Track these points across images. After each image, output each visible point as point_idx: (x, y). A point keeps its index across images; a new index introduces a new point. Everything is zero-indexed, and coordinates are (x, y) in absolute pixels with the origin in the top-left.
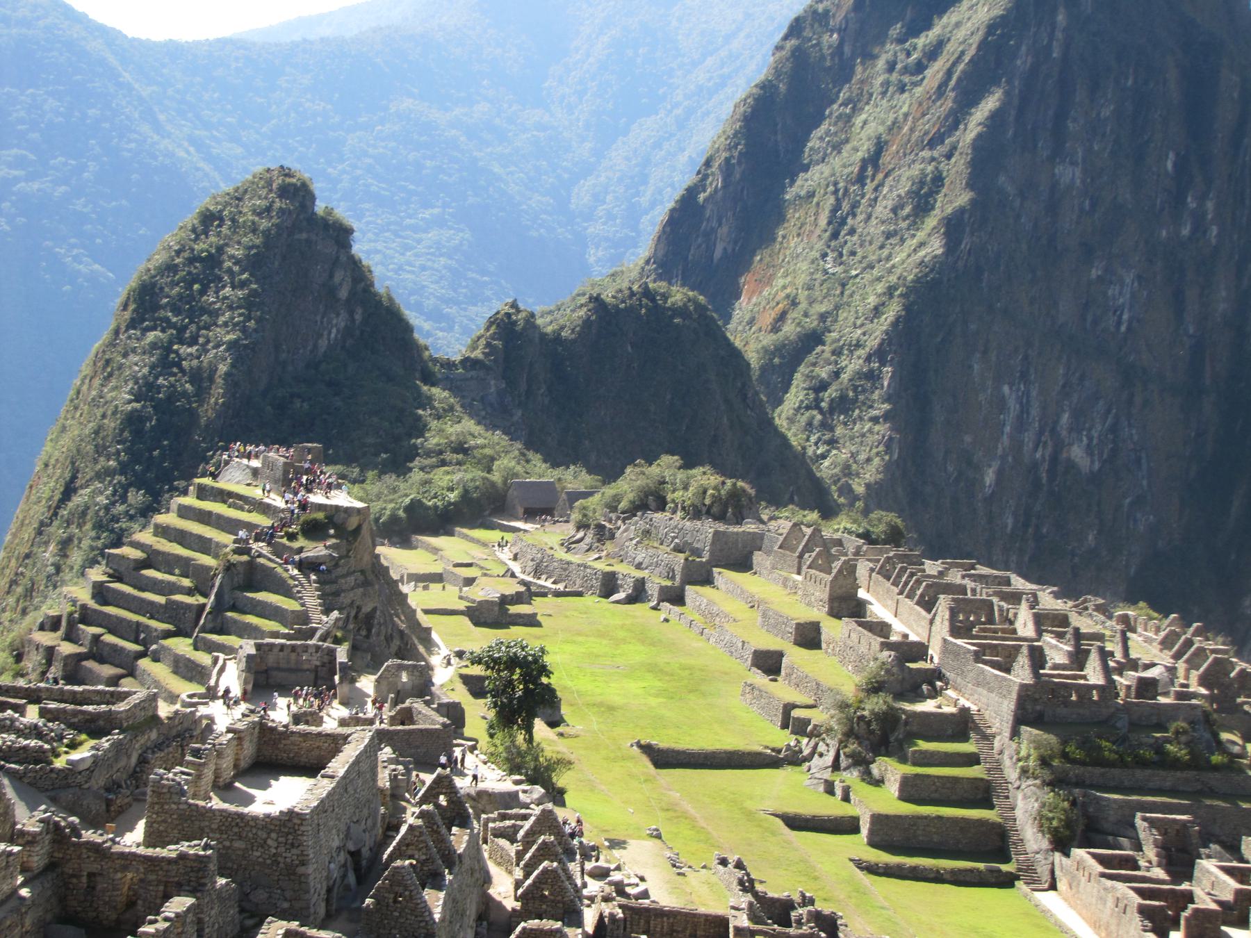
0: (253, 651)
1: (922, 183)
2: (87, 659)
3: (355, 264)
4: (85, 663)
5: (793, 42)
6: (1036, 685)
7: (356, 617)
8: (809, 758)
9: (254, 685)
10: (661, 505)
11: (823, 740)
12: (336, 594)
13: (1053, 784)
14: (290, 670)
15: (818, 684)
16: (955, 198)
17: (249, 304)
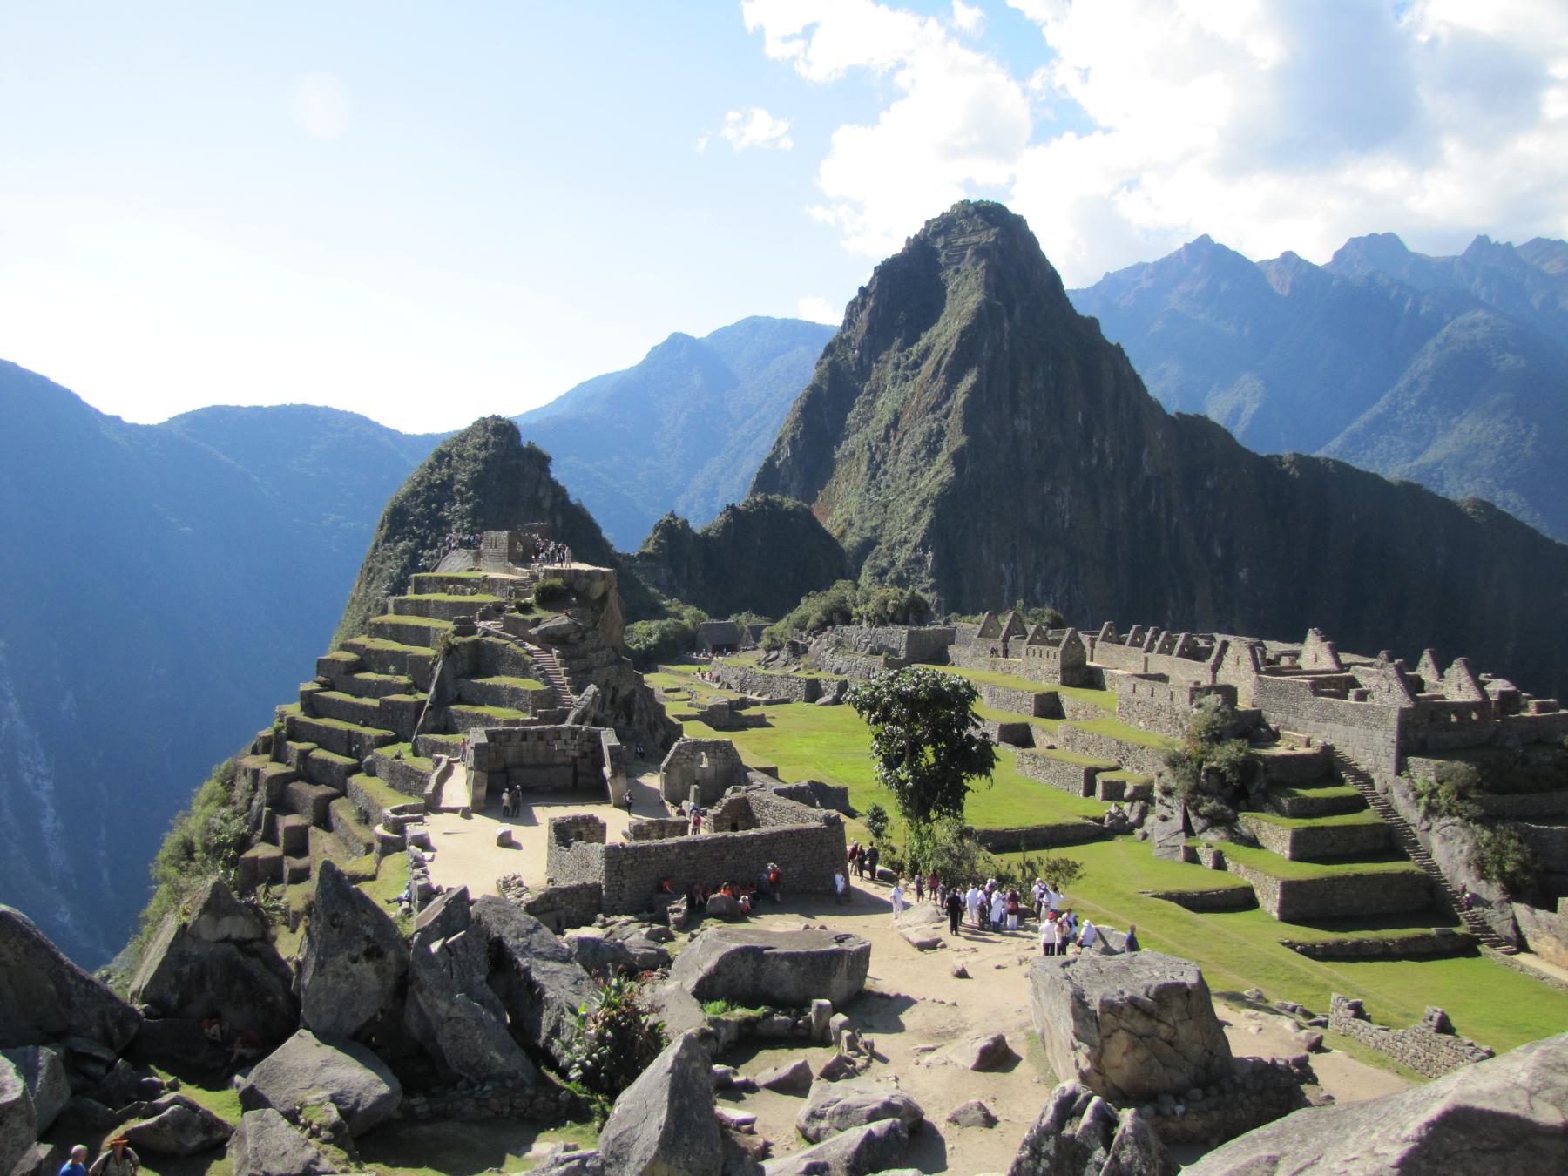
0: (484, 740)
1: (931, 435)
2: (295, 780)
3: (554, 484)
4: (293, 786)
5: (829, 358)
6: (1416, 706)
7: (613, 701)
8: (1140, 822)
9: (488, 790)
10: (847, 619)
11: (1161, 801)
12: (587, 671)
13: (1486, 820)
14: (539, 766)
15: (1120, 743)
16: (955, 440)
17: (474, 514)
